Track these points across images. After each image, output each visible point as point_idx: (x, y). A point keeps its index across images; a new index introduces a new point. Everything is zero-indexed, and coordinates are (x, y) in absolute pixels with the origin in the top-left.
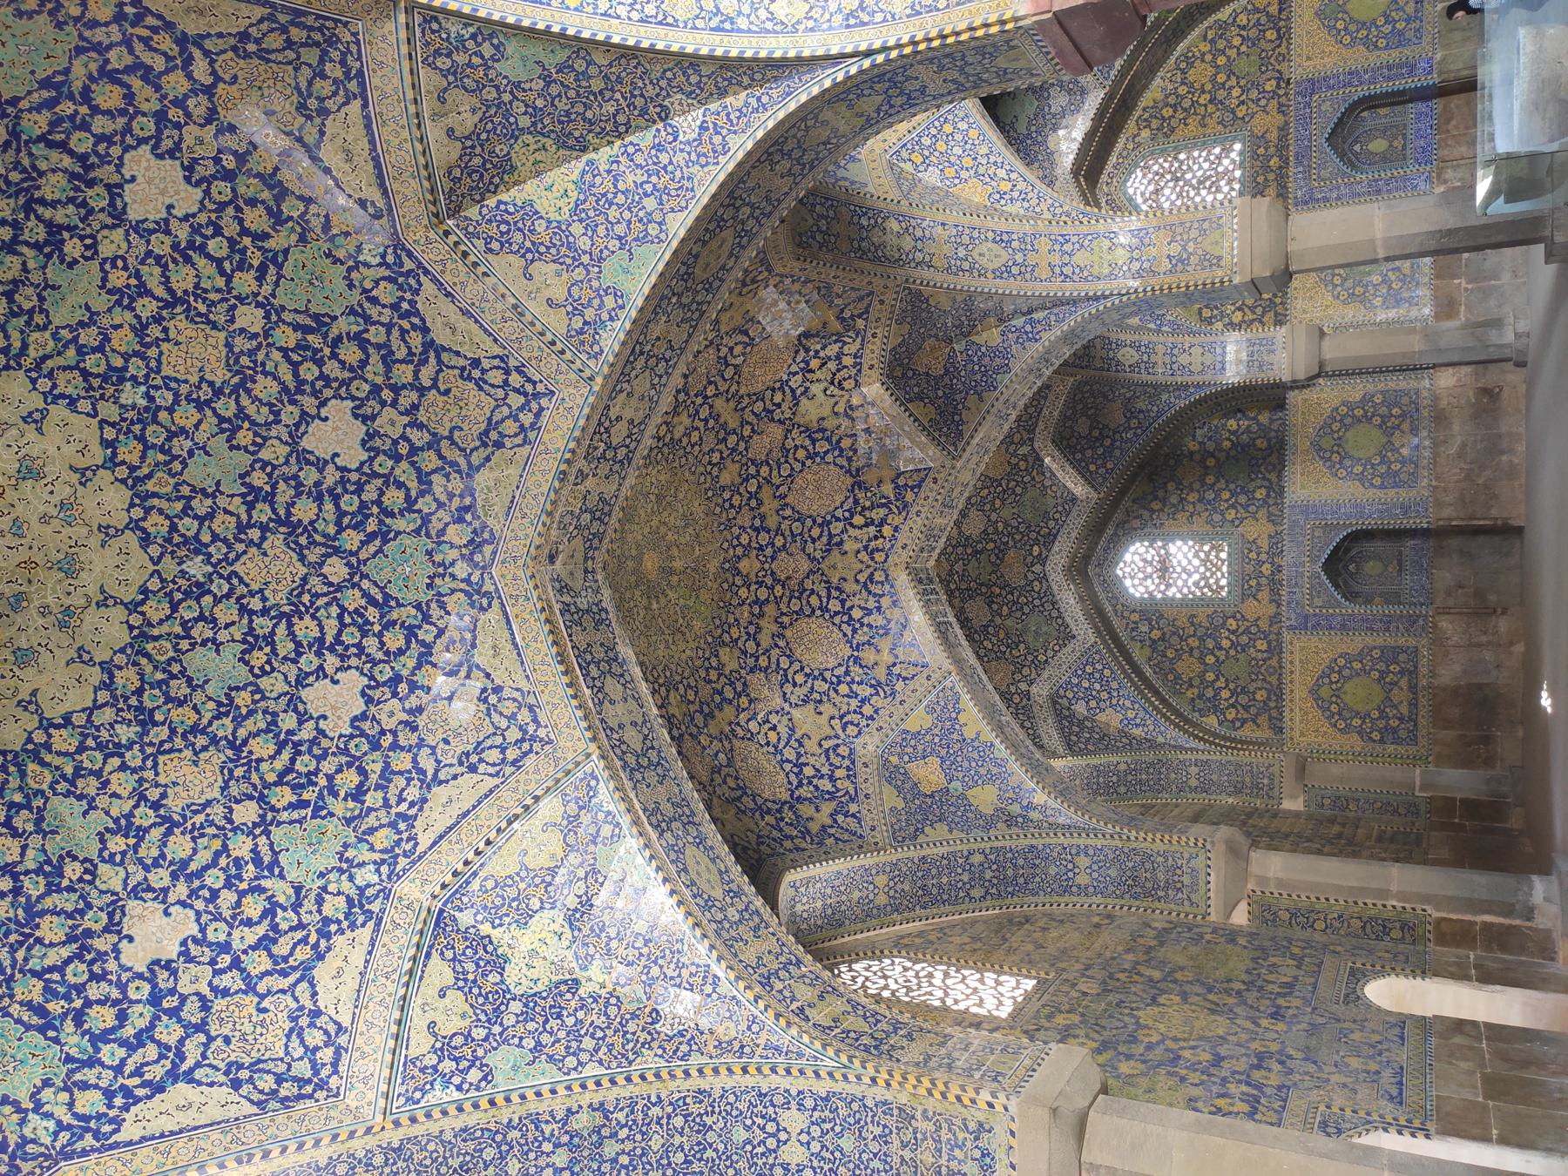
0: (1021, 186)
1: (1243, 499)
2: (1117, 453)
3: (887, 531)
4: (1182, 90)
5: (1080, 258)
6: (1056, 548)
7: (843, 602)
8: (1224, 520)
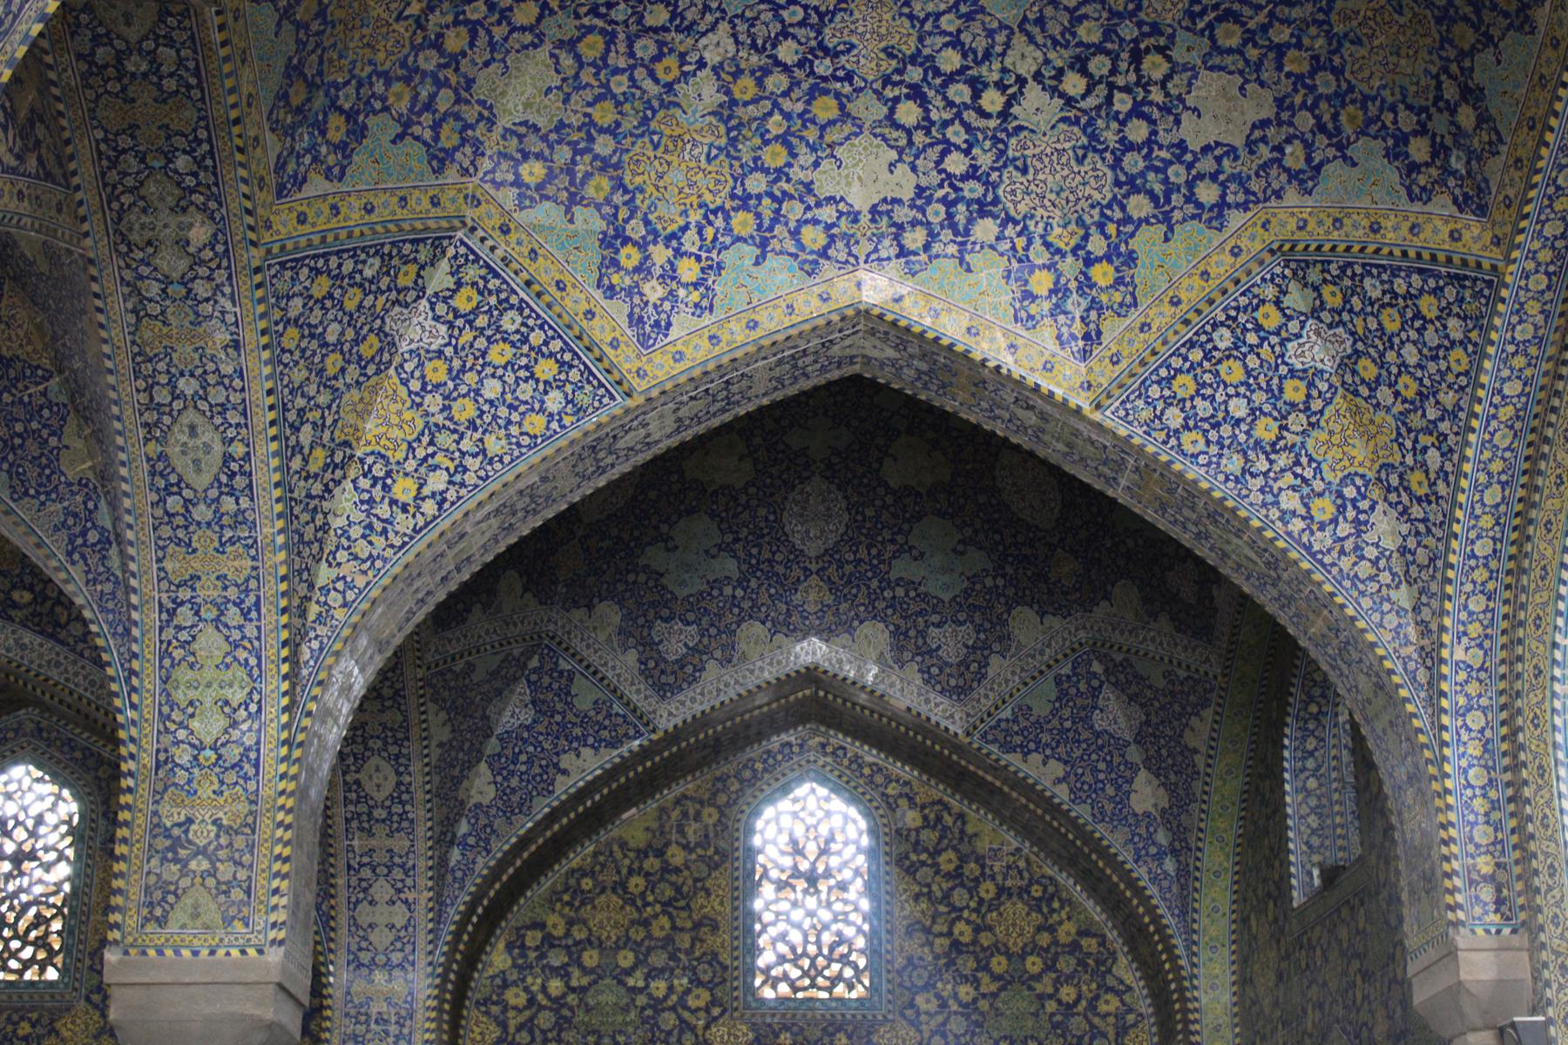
0: (404, 523)
4: (987, 890)
5: (210, 643)
6: (27, 637)
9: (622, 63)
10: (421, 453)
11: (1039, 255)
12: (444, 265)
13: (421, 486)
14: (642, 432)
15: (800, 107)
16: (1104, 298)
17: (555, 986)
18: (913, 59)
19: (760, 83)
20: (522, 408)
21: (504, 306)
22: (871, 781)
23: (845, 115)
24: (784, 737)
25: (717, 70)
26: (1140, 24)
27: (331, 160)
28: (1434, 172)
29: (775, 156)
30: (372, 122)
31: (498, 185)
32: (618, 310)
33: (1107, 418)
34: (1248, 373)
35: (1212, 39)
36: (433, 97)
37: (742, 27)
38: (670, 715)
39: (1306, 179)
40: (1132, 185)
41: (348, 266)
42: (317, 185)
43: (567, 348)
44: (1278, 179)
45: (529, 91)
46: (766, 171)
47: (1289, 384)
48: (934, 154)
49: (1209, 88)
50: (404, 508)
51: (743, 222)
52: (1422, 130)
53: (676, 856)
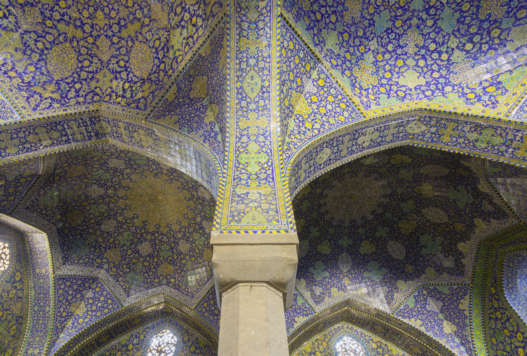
3: (119, 99)
7: (85, 80)
10: (312, 118)
13: (313, 126)
15: (393, 63)
20: (338, 114)
23: (405, 64)
25: (373, 51)
29: (388, 75)
37: (379, 40)
46: (386, 79)
48: (429, 73)
50: (309, 130)
51: (382, 90)
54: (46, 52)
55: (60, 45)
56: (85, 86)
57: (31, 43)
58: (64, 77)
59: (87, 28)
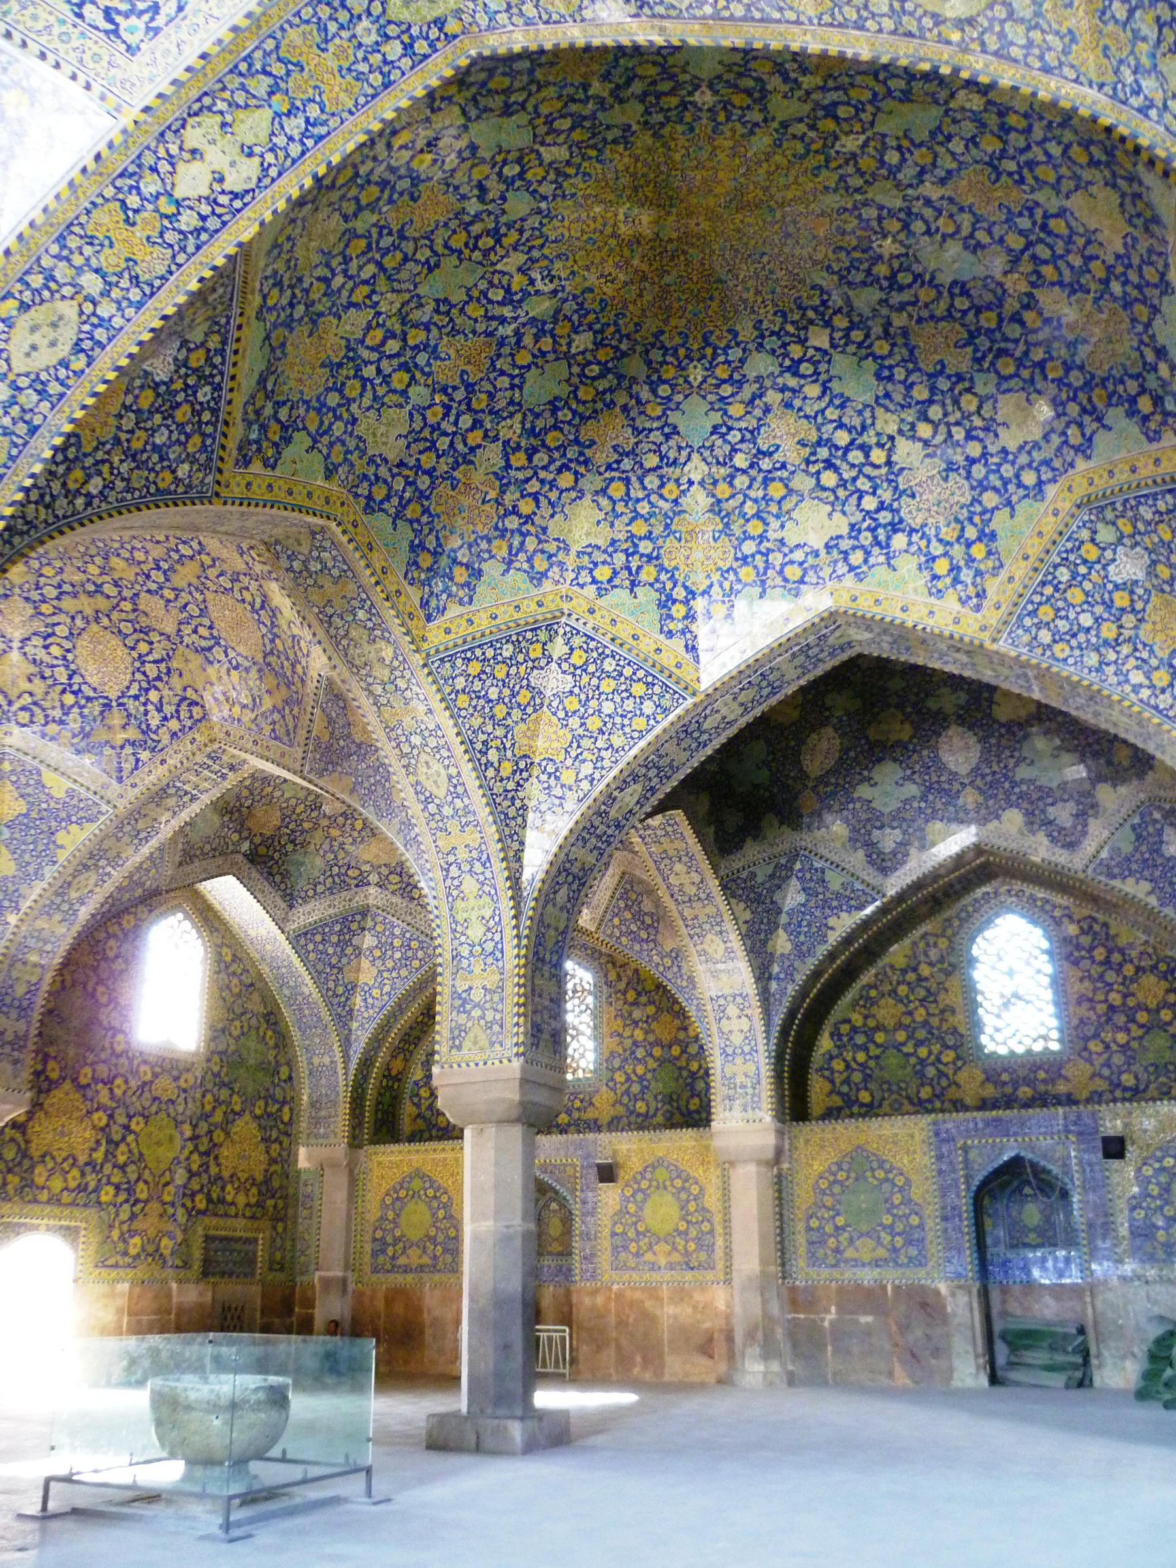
1: (636, 1088)
2: (637, 947)
4: (1129, 970)
5: (470, 885)
7: (159, 678)
8: (613, 1070)
9: (641, 494)
11: (937, 549)
12: (559, 640)
14: (718, 717)
15: (761, 493)
16: (982, 567)
17: (861, 1057)
18: (819, 443)
19: (731, 484)
21: (603, 656)
22: (1042, 908)
23: (790, 491)
24: (984, 889)
25: (702, 483)
26: (949, 377)
27: (461, 593)
28: (1158, 417)
29: (755, 528)
30: (484, 566)
31: (582, 586)
32: (678, 644)
33: (1003, 646)
34: (1087, 594)
35: (997, 372)
36: (522, 543)
37: (707, 453)
38: (894, 884)
39: (1085, 448)
40: (982, 486)
41: (490, 653)
42: (454, 610)
43: (648, 674)
44: (1069, 455)
45: (586, 526)
47: (1117, 596)
48: (853, 500)
49: (1007, 407)
51: (747, 573)
52: (1143, 390)
53: (925, 970)
54: (70, 656)
55: (85, 635)
56: (166, 692)
57: (41, 654)
58: (122, 687)
59: (109, 589)
